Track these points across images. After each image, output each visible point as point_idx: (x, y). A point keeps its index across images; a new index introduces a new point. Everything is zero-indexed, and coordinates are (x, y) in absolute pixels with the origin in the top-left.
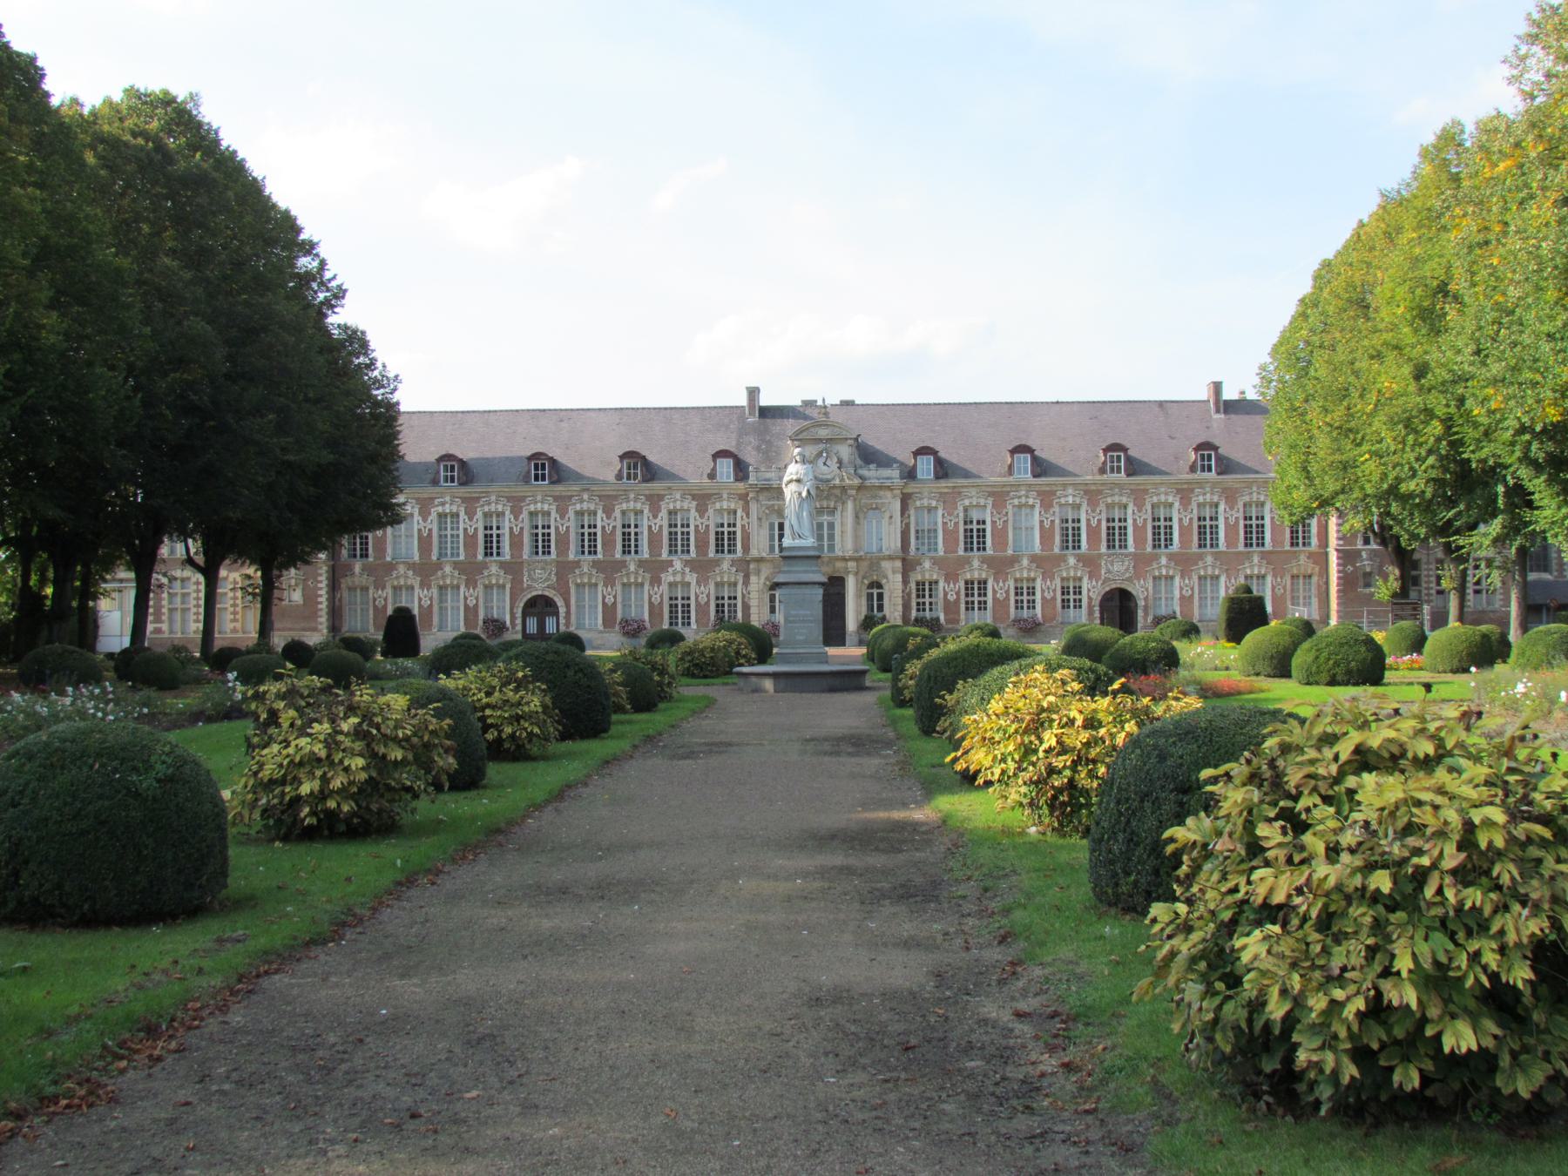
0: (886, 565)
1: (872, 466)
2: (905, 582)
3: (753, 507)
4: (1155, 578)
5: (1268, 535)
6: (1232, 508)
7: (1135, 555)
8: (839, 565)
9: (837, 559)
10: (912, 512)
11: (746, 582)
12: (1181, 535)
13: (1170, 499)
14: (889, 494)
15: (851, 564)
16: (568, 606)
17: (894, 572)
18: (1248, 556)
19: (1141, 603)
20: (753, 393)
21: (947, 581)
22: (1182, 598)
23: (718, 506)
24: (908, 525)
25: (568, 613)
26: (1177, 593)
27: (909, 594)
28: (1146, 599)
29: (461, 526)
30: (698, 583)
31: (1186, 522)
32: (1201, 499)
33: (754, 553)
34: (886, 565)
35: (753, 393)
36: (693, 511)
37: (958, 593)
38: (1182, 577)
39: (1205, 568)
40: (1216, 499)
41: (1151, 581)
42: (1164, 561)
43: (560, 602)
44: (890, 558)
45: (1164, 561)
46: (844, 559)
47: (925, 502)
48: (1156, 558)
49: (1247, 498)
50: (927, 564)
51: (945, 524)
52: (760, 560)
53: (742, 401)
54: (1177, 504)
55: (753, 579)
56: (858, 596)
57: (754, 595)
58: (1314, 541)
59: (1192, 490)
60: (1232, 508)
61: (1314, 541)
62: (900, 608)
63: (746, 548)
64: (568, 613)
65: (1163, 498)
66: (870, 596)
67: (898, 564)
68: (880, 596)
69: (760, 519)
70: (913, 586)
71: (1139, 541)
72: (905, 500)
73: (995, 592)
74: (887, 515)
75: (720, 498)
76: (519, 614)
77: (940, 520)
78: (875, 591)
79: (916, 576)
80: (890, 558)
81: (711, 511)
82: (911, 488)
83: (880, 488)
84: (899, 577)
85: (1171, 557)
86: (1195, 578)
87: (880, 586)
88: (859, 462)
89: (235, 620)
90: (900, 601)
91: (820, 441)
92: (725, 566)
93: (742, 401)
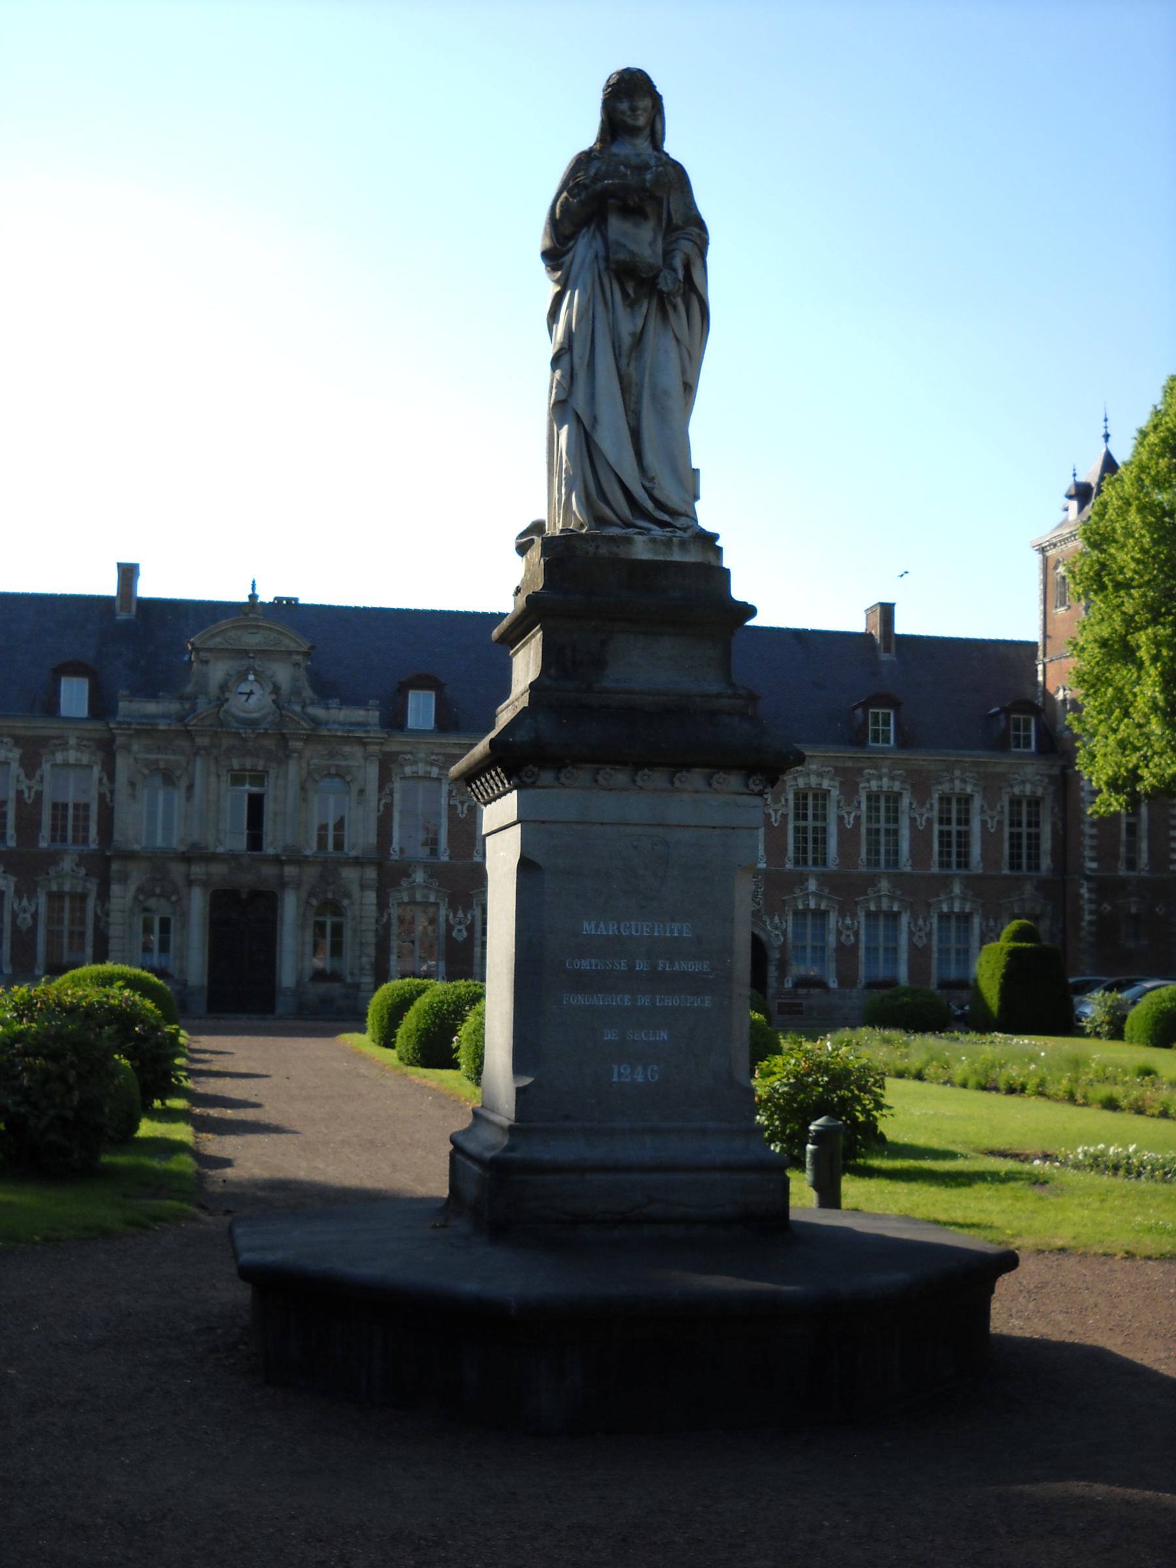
0: (350, 874)
1: (334, 702)
2: (382, 905)
3: (123, 764)
4: (796, 913)
5: (976, 851)
6: (922, 803)
7: (765, 872)
9: (267, 860)
10: (397, 785)
11: (104, 896)
12: (840, 843)
13: (826, 784)
14: (358, 751)
15: (290, 871)
17: (363, 887)
18: (944, 883)
19: (775, 955)
20: (128, 573)
21: (453, 907)
22: (841, 947)
23: (59, 757)
24: (389, 808)
26: (832, 940)
28: (783, 948)
30: (19, 893)
31: (850, 822)
32: (874, 785)
34: (350, 874)
35: (128, 573)
36: (15, 767)
38: (842, 914)
39: (878, 899)
40: (897, 786)
41: (790, 918)
42: (812, 885)
44: (358, 862)
45: (812, 885)
46: (277, 860)
47: (421, 769)
48: (802, 880)
49: (946, 787)
50: (419, 877)
51: (452, 808)
52: (129, 856)
54: (835, 793)
55: (116, 889)
56: (302, 927)
57: (115, 917)
58: (1046, 862)
59: (860, 771)
60: (922, 803)
61: (1046, 862)
62: (371, 950)
65: (814, 781)
66: (320, 927)
67: (371, 873)
68: (337, 930)
69: (132, 784)
71: (775, 850)
72: (387, 765)
74: (355, 788)
75: (65, 746)
77: (444, 801)
80: (358, 862)
81: (46, 767)
82: (396, 744)
83: (346, 740)
84: (371, 897)
85: (823, 880)
86: (862, 915)
87: (337, 910)
88: (308, 693)
90: (371, 938)
91: (243, 653)
92: (67, 864)
93: (109, 587)
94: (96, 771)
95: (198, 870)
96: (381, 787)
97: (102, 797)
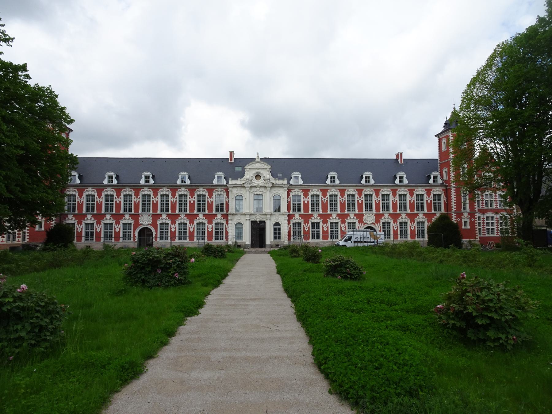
8: (263, 217)
11: (227, 223)
14: (282, 189)
16: (156, 232)
20: (231, 153)
24: (290, 201)
25: (156, 234)
27: (290, 228)
29: (77, 200)
33: (230, 211)
35: (231, 153)
37: (309, 228)
43: (153, 230)
46: (266, 214)
53: (228, 156)
55: (230, 222)
63: (227, 211)
64: (156, 234)
66: (275, 229)
67: (286, 216)
68: (279, 229)
70: (291, 224)
73: (323, 228)
76: (136, 234)
78: (277, 227)
79: (293, 221)
89: (19, 237)
93: (228, 156)
94: (225, 195)
95: (248, 217)
96: (288, 197)
97: (226, 201)
